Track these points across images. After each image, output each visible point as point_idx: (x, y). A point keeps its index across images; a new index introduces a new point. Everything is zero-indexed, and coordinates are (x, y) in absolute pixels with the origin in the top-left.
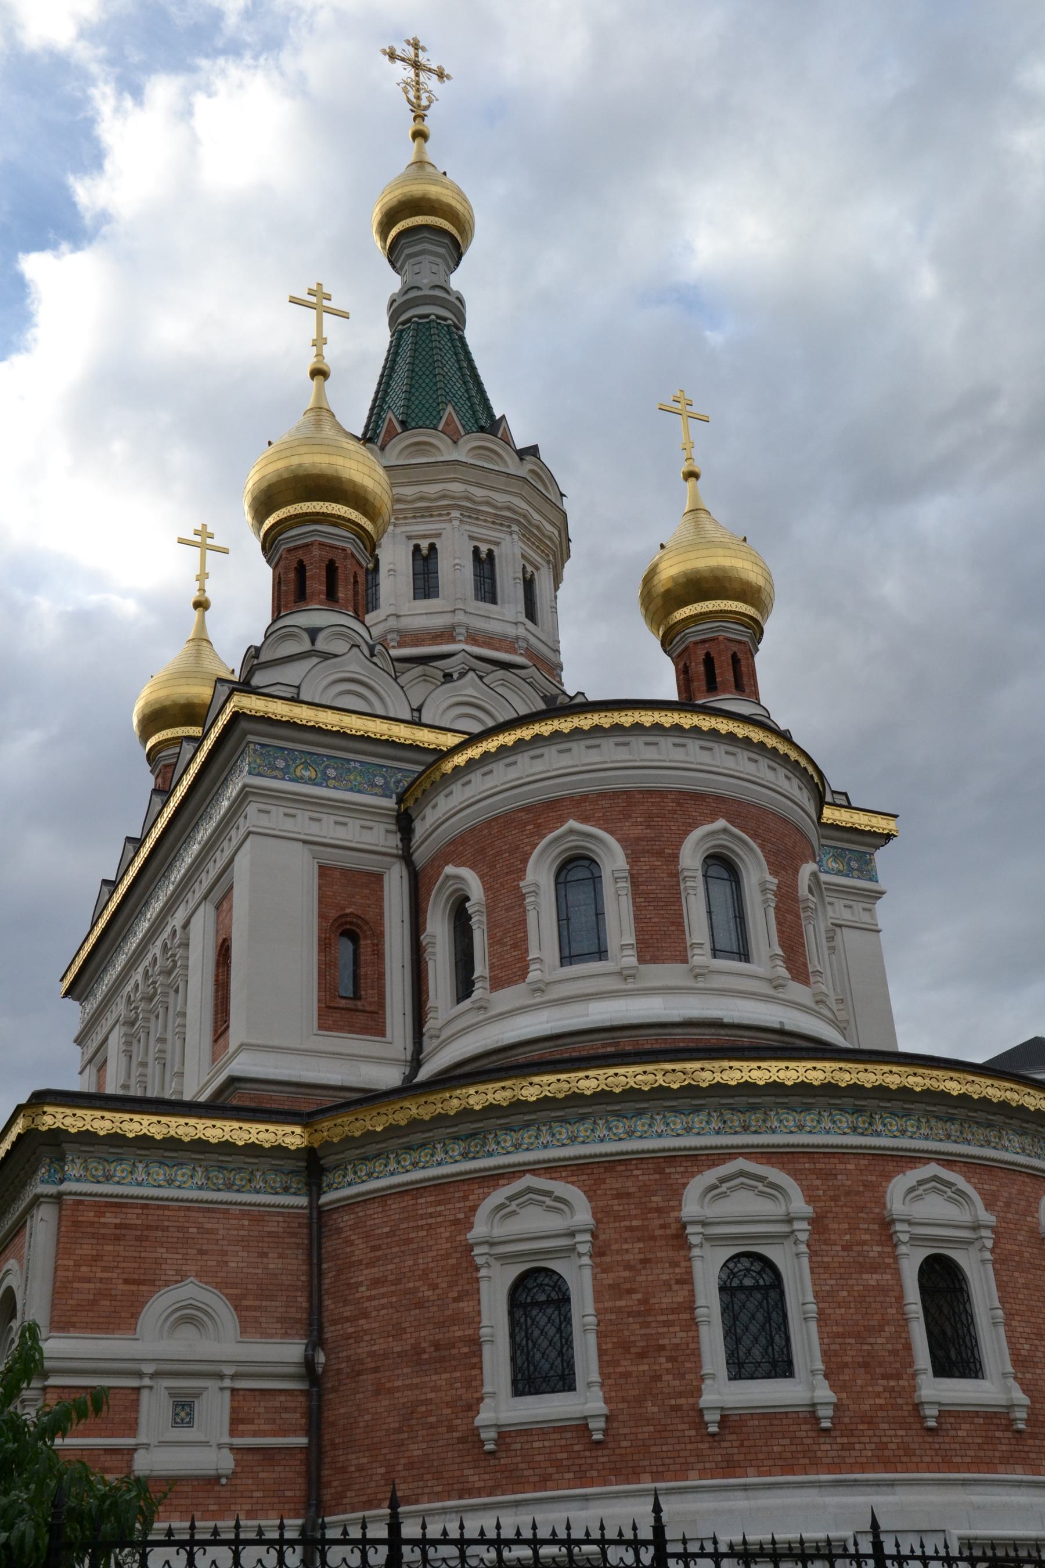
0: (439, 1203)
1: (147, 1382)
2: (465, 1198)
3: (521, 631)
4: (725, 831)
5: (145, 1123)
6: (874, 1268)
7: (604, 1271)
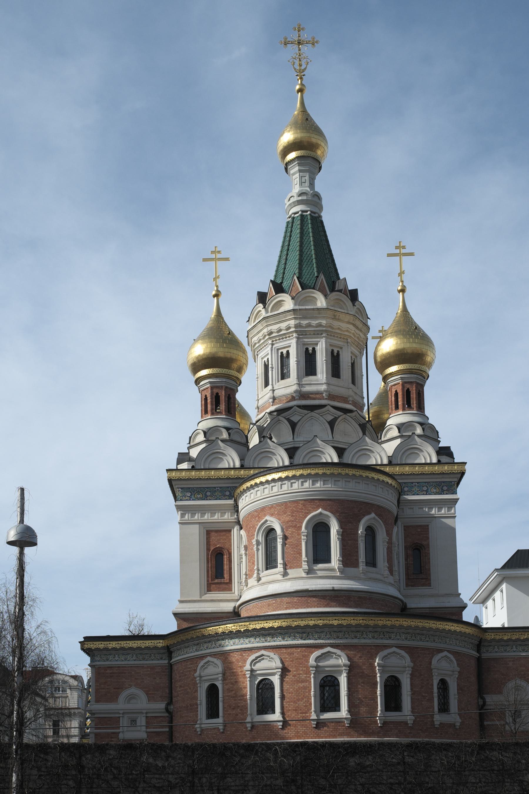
0: (191, 664)
1: (121, 715)
2: (196, 663)
4: (321, 514)
5: (114, 644)
6: (302, 682)
7: (226, 685)
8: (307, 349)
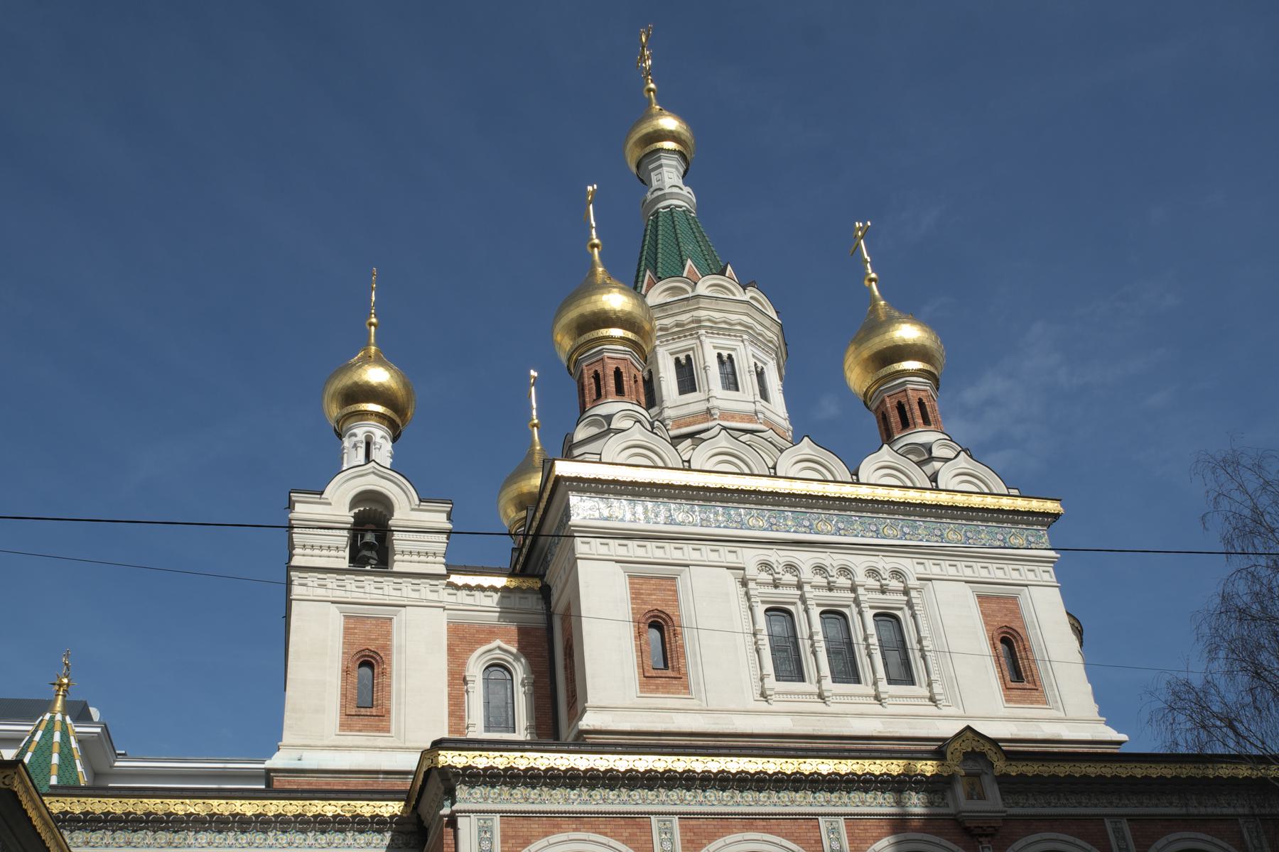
3: (759, 407)
8: (719, 356)
